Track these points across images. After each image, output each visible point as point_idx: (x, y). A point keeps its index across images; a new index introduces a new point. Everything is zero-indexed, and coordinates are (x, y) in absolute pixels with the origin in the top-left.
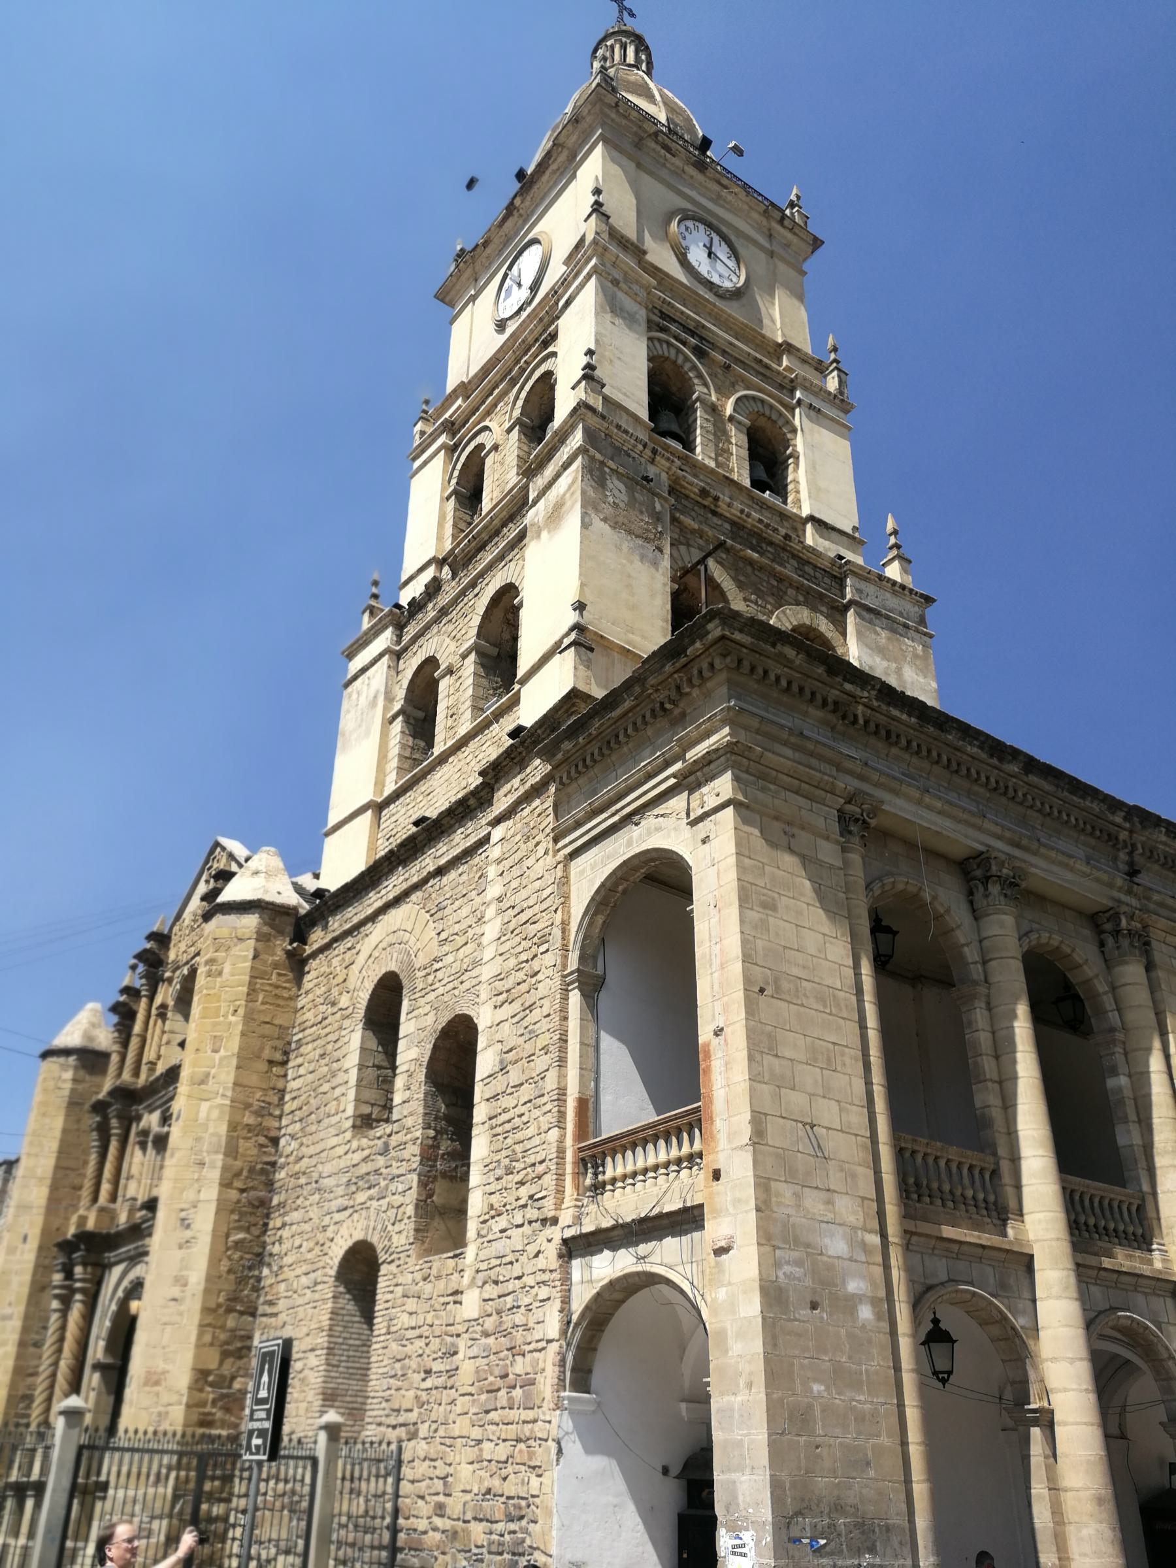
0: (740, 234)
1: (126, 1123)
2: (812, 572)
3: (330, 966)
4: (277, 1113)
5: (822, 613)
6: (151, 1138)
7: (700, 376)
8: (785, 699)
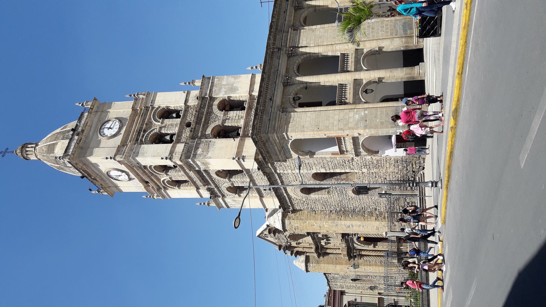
0: (99, 120)
1: (323, 248)
2: (203, 105)
3: (296, 204)
4: (325, 211)
5: (213, 103)
6: (327, 242)
7: (152, 131)
8: (263, 123)
